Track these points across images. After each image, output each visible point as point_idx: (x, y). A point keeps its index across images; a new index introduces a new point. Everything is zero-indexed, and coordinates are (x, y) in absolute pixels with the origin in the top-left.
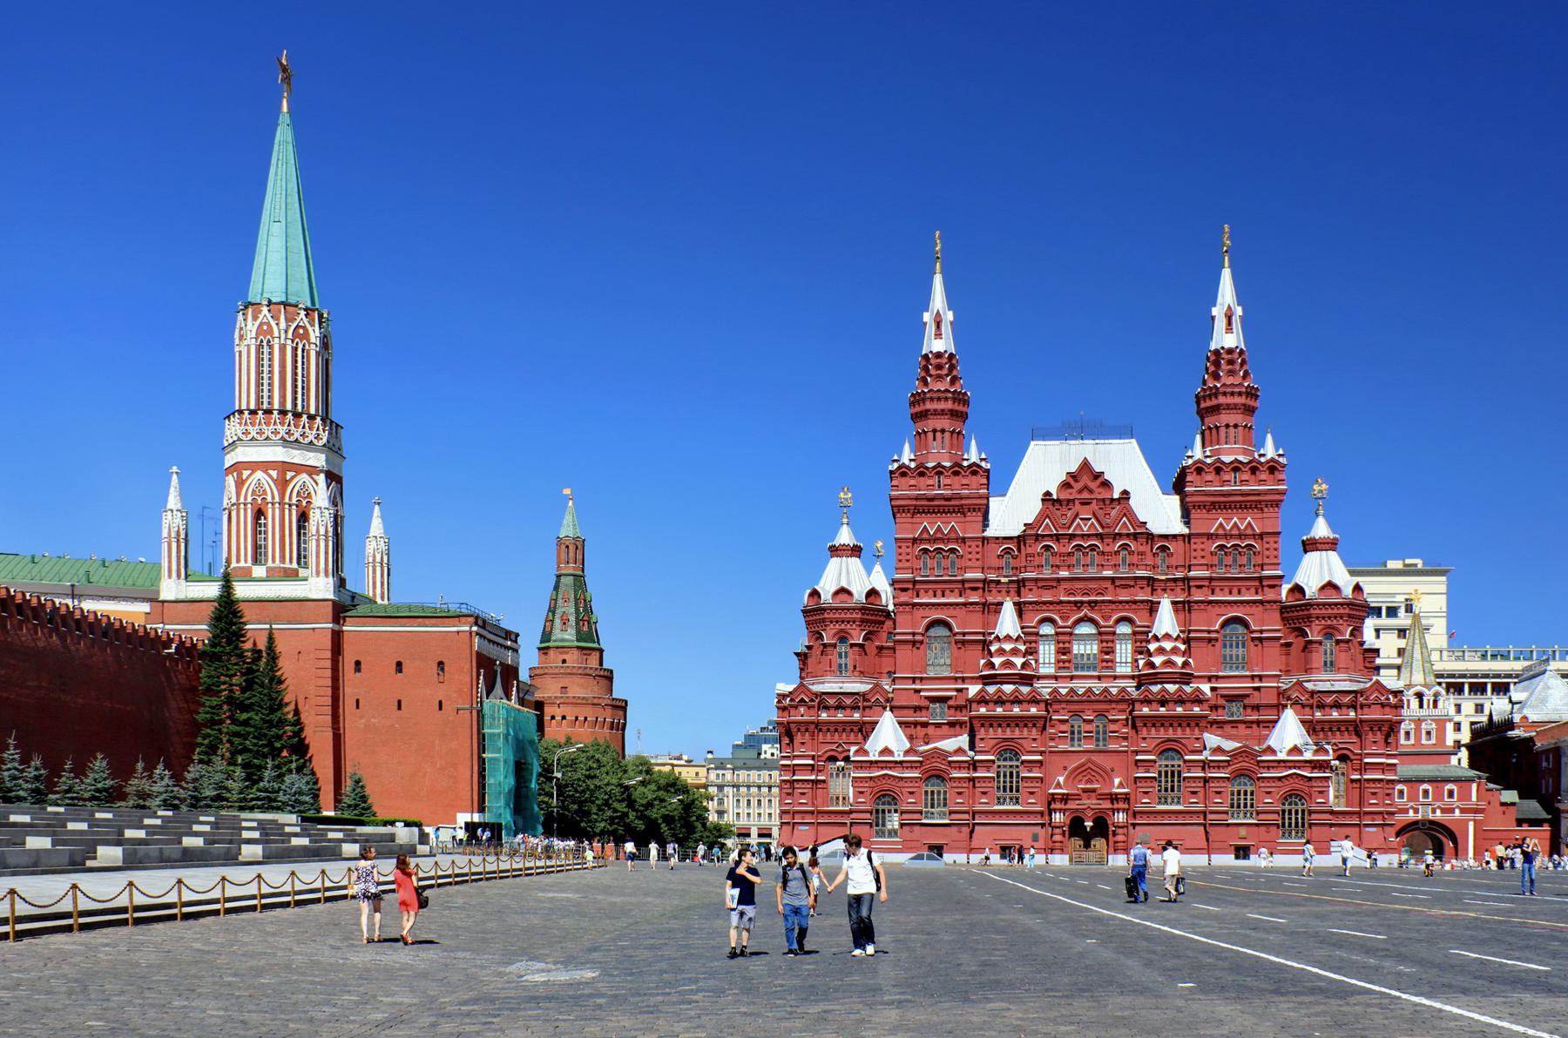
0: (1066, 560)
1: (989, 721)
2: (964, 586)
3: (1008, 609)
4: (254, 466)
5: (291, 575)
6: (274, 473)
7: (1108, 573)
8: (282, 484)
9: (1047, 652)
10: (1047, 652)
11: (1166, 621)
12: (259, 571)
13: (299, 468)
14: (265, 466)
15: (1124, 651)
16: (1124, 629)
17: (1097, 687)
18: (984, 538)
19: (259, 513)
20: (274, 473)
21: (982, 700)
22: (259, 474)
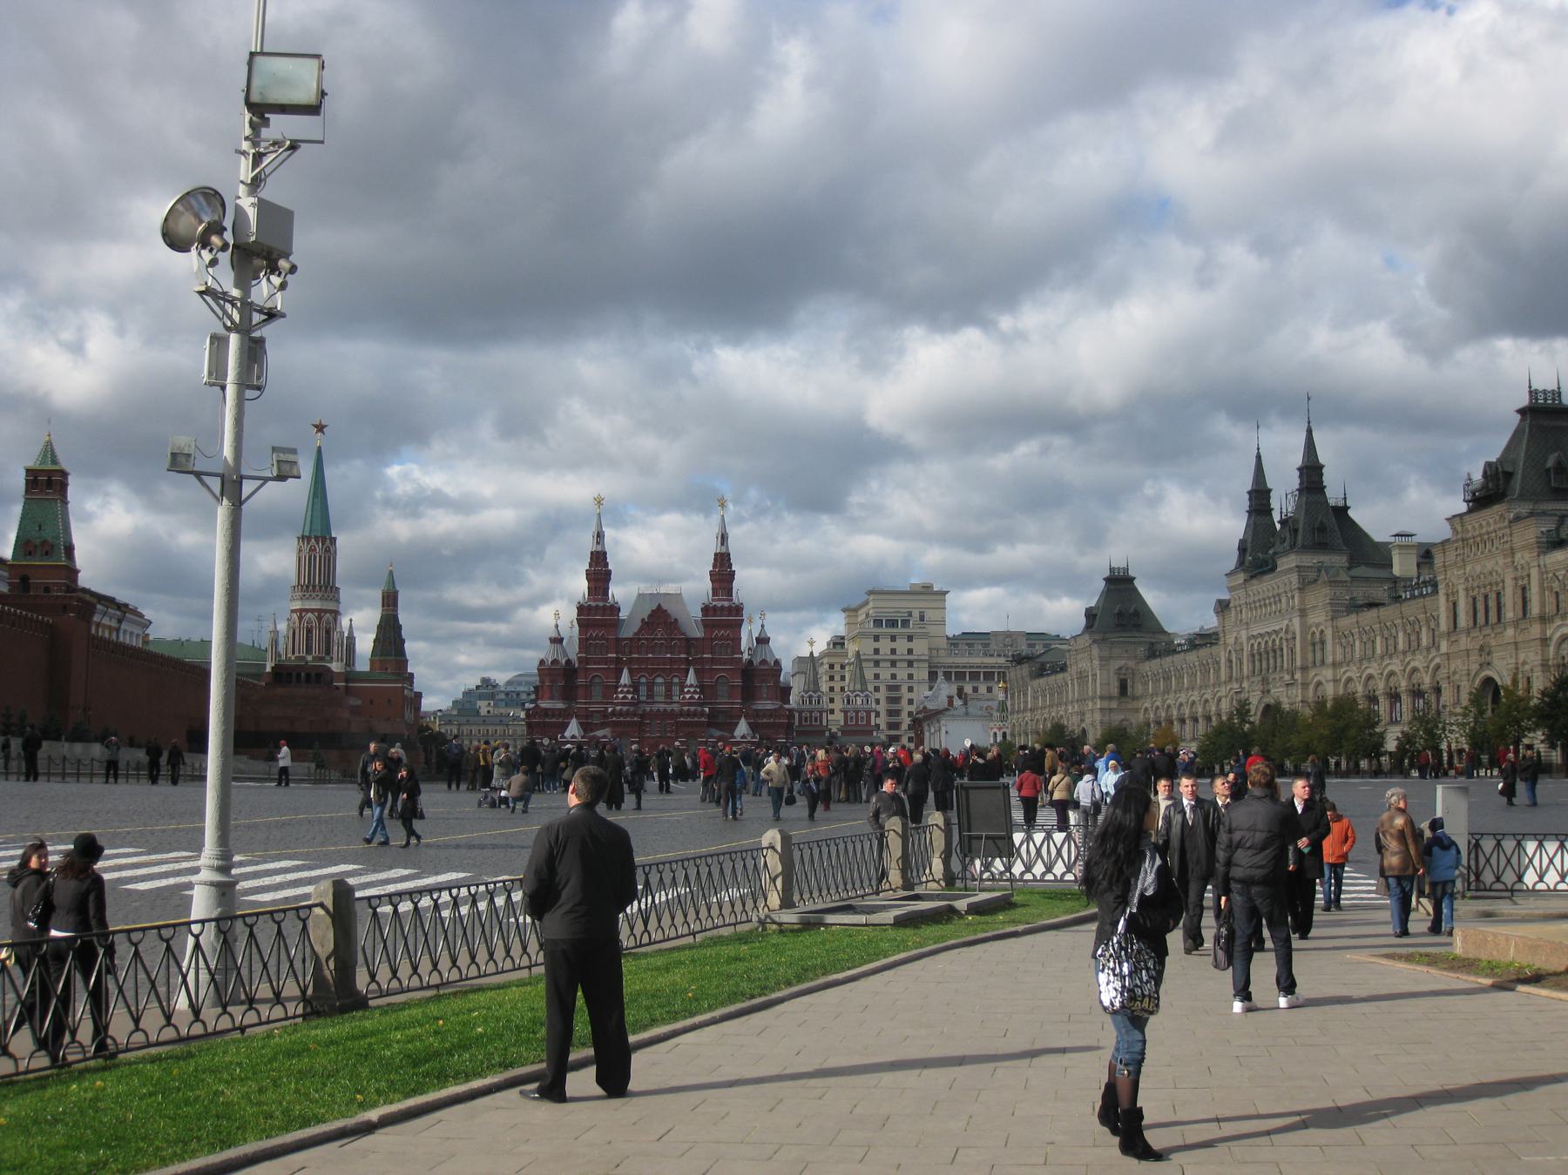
0: (652, 649)
2: (607, 661)
3: (625, 672)
4: (307, 611)
8: (319, 618)
9: (643, 690)
10: (643, 690)
11: (691, 679)
13: (326, 611)
14: (312, 611)
15: (676, 689)
16: (676, 680)
17: (662, 707)
18: (618, 640)
19: (309, 631)
21: (613, 713)
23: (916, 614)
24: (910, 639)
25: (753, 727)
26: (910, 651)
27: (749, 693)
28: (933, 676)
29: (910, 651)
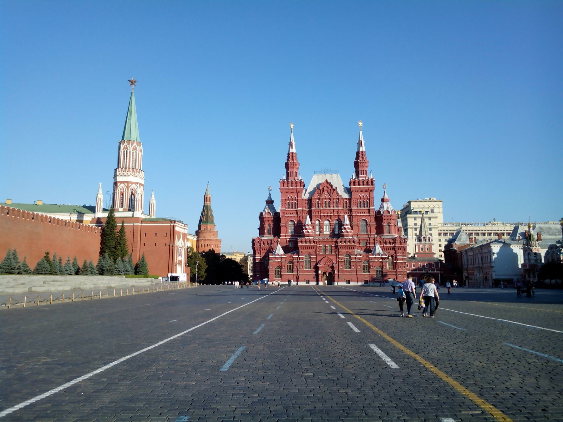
1: (303, 247)
5: (130, 210)
6: (126, 184)
7: (332, 208)
8: (128, 187)
9: (317, 227)
12: (121, 209)
13: (133, 183)
14: (124, 182)
20: (126, 184)
22: (122, 185)
23: (430, 210)
24: (430, 219)
25: (383, 249)
26: (430, 224)
27: (380, 230)
28: (440, 234)
29: (430, 224)
